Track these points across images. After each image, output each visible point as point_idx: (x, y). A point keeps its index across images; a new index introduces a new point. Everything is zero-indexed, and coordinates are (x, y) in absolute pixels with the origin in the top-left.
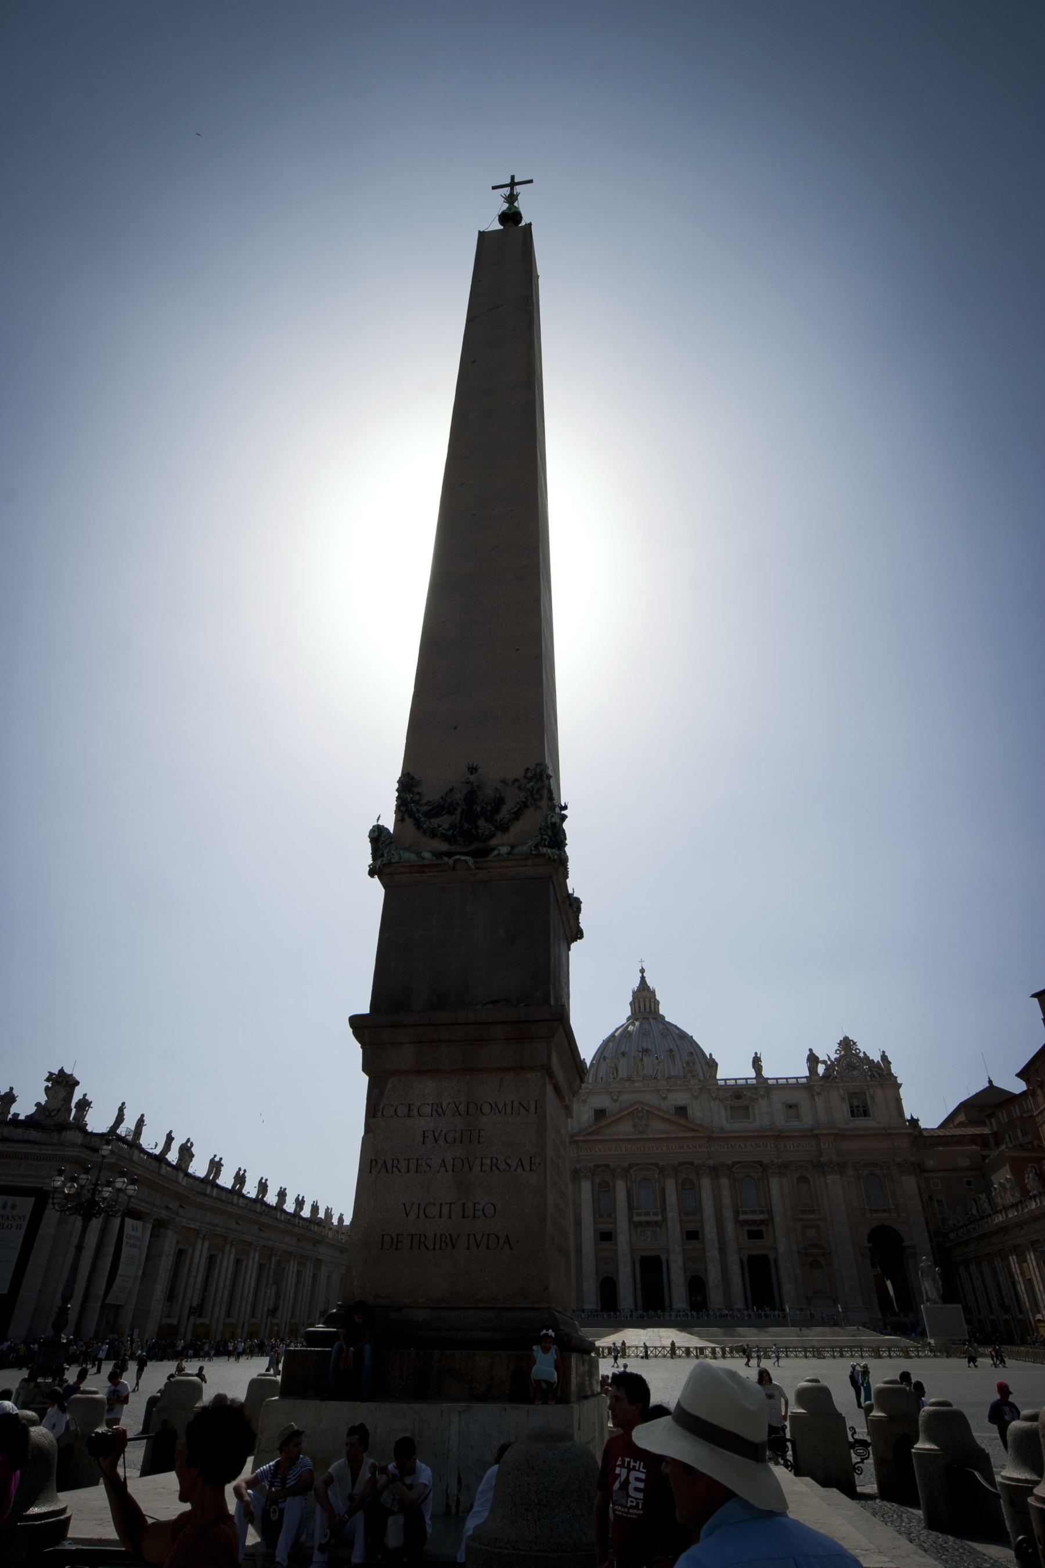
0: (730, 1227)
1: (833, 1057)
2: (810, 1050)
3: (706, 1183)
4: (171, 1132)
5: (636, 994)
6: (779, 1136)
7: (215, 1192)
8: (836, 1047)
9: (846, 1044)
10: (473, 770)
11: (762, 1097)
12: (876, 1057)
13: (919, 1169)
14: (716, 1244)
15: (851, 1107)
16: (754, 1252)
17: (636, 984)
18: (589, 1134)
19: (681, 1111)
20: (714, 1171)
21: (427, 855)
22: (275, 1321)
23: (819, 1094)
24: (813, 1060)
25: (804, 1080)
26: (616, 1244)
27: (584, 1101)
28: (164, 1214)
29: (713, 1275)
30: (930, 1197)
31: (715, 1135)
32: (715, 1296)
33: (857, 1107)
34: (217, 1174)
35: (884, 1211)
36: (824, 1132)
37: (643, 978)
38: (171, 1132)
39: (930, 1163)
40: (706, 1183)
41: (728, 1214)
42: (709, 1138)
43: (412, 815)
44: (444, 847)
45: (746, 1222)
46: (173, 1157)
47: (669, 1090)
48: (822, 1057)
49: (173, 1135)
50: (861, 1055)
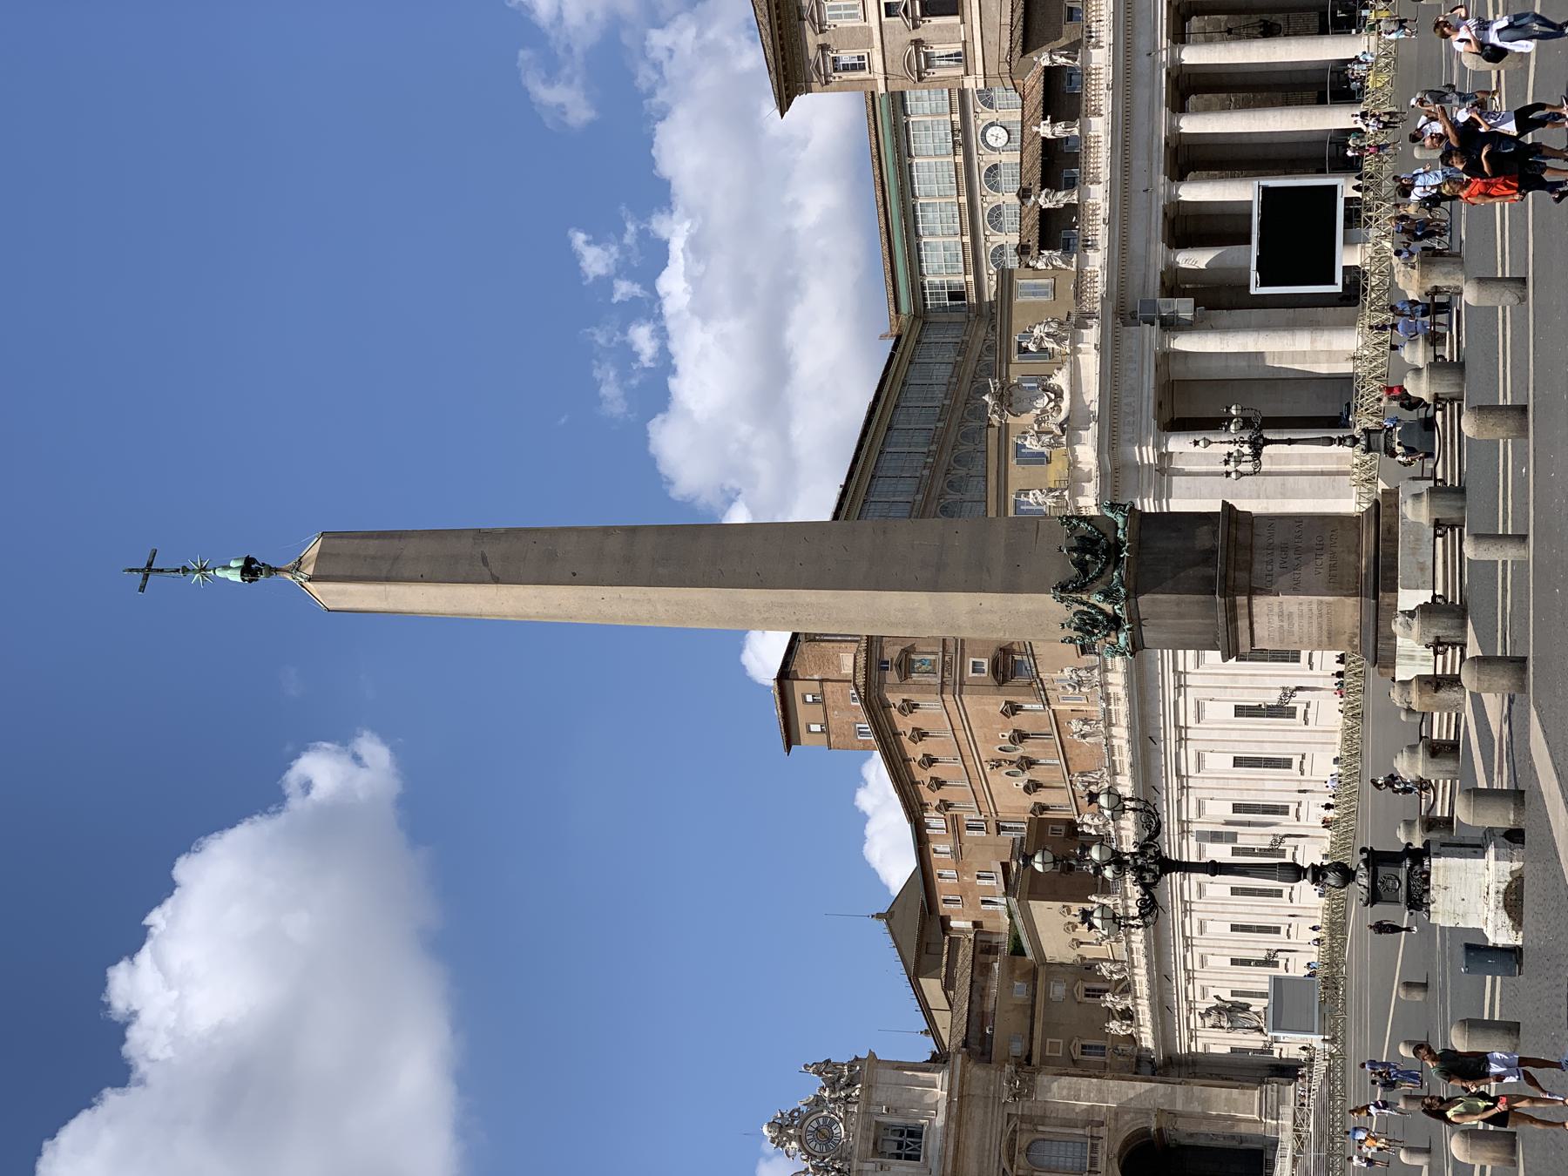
15: (899, 1157)
30: (1075, 1062)
33: (900, 1146)
35: (1094, 1146)
39: (1018, 1048)
43: (1085, 584)
44: (1111, 567)
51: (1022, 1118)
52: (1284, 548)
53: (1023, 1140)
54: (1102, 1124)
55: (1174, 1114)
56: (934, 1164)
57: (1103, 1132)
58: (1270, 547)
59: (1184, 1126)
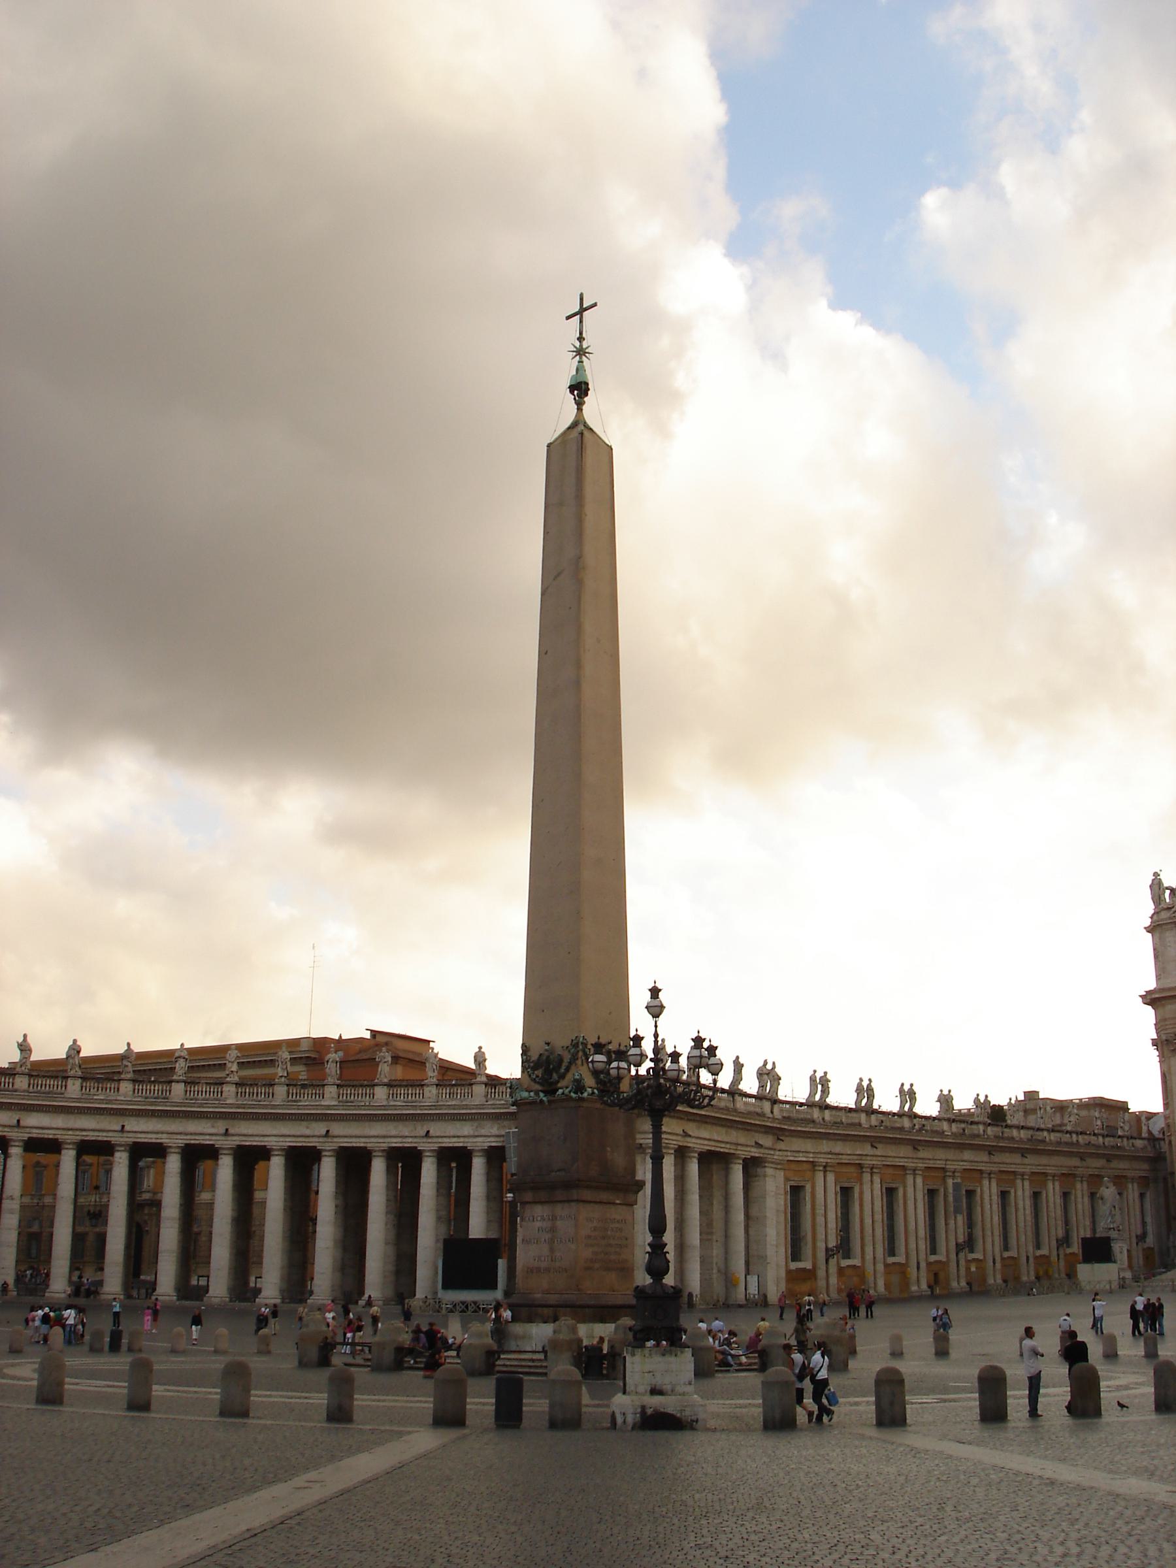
4: (738, 1058)
7: (827, 1114)
10: (548, 1044)
21: (532, 1094)
22: (971, 1256)
28: (755, 1152)
34: (825, 1091)
38: (738, 1058)
46: (750, 1084)
49: (741, 1061)
52: (553, 1230)
58: (554, 1218)
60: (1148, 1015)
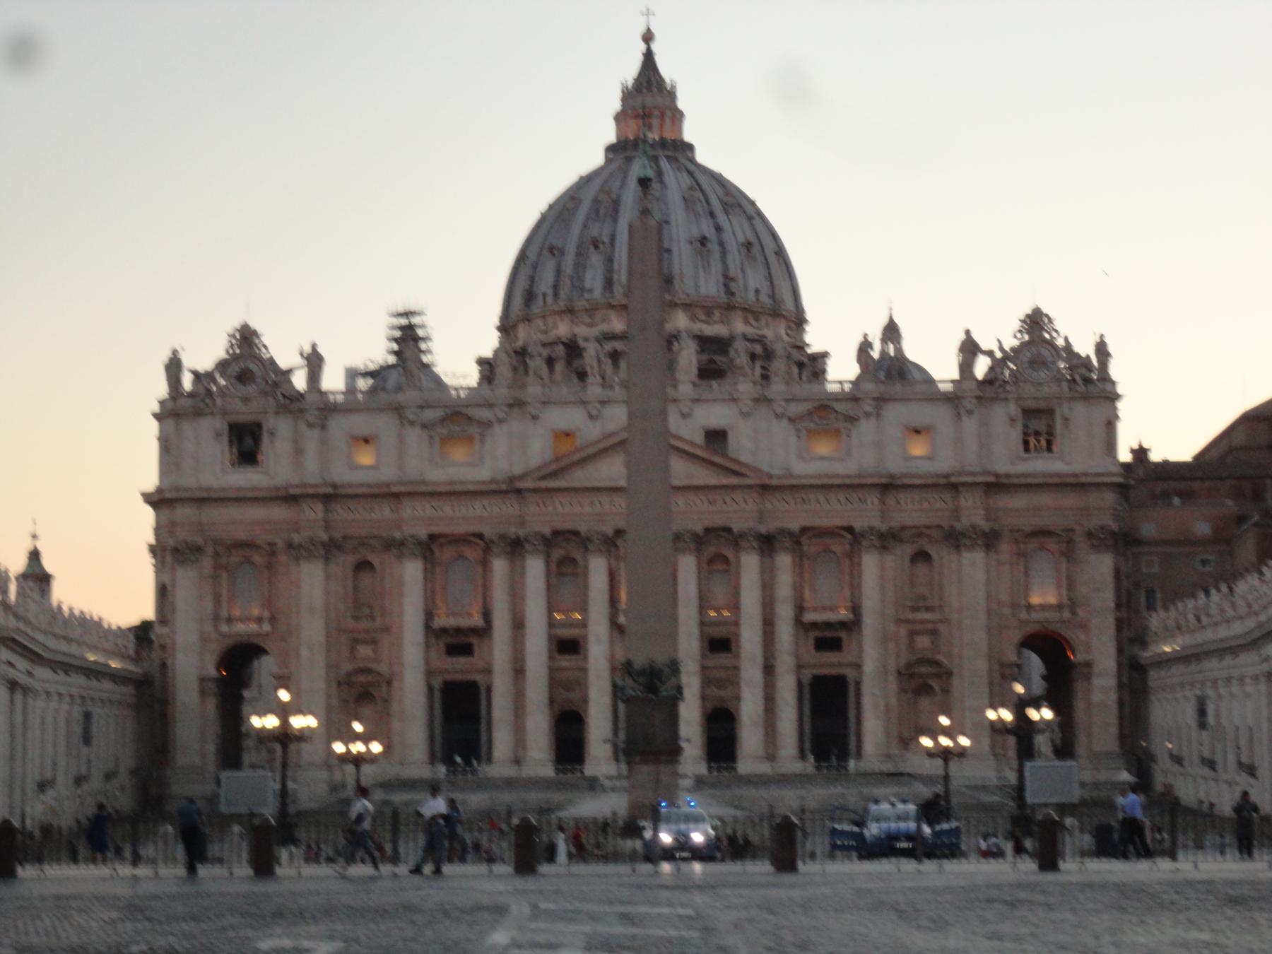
0: (785, 632)
1: (1010, 343)
2: (968, 332)
3: (750, 564)
5: (628, 96)
6: (889, 486)
8: (1017, 325)
9: (1036, 322)
11: (867, 415)
12: (1084, 348)
13: (1123, 541)
14: (760, 659)
15: (1026, 434)
16: (824, 671)
17: (630, 70)
18: (543, 478)
19: (716, 437)
20: (768, 544)
23: (970, 412)
24: (970, 349)
25: (948, 387)
26: (585, 659)
27: (535, 418)
29: (750, 708)
31: (775, 482)
32: (750, 738)
33: (1037, 434)
36: (969, 479)
37: (649, 58)
39: (1148, 530)
40: (750, 564)
41: (785, 613)
42: (765, 489)
45: (814, 625)
47: (696, 401)
48: (984, 346)
50: (1060, 342)
51: (1070, 542)
53: (1052, 545)
54: (1073, 612)
55: (1088, 677)
56: (1020, 468)
57: (1067, 614)
59: (1079, 686)
60: (148, 515)
